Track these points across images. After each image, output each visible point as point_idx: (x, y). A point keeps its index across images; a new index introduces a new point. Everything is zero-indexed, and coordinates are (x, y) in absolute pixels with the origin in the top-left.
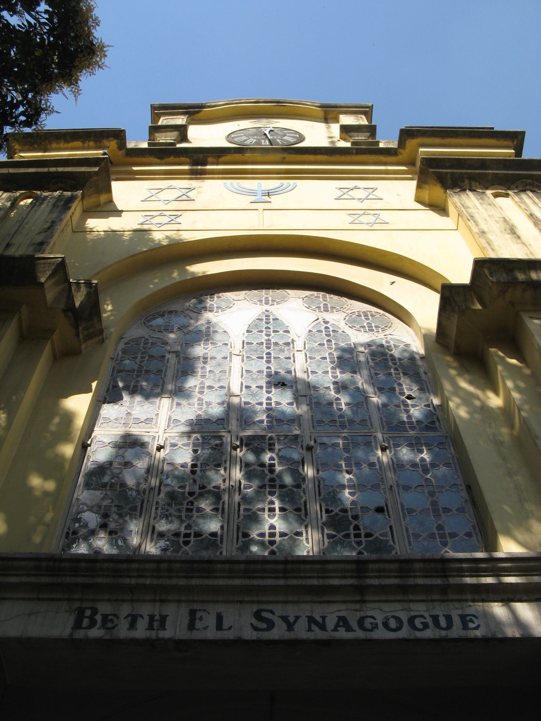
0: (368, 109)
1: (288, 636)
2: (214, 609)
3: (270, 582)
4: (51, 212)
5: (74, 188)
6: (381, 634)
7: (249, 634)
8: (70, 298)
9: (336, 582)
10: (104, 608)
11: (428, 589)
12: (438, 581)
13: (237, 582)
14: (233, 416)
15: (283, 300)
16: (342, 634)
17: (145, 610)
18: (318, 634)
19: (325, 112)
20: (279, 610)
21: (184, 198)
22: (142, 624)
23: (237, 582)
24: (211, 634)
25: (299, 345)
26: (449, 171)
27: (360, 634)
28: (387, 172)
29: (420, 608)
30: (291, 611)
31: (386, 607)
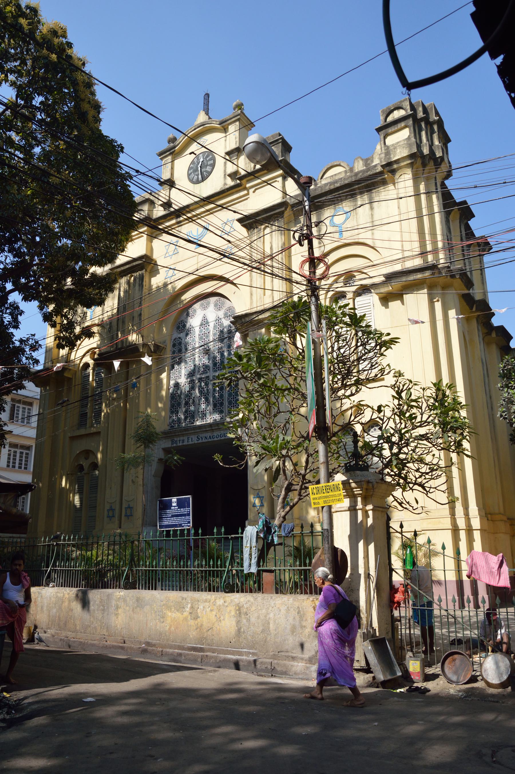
2: (191, 437)
3: (198, 431)
4: (139, 290)
5: (141, 269)
6: (216, 439)
7: (196, 442)
8: (150, 349)
10: (175, 439)
14: (197, 369)
15: (208, 304)
16: (210, 440)
17: (181, 438)
18: (206, 440)
20: (200, 435)
22: (181, 442)
24: (191, 443)
25: (211, 333)
26: (247, 222)
27: (212, 440)
30: (203, 435)
31: (217, 432)
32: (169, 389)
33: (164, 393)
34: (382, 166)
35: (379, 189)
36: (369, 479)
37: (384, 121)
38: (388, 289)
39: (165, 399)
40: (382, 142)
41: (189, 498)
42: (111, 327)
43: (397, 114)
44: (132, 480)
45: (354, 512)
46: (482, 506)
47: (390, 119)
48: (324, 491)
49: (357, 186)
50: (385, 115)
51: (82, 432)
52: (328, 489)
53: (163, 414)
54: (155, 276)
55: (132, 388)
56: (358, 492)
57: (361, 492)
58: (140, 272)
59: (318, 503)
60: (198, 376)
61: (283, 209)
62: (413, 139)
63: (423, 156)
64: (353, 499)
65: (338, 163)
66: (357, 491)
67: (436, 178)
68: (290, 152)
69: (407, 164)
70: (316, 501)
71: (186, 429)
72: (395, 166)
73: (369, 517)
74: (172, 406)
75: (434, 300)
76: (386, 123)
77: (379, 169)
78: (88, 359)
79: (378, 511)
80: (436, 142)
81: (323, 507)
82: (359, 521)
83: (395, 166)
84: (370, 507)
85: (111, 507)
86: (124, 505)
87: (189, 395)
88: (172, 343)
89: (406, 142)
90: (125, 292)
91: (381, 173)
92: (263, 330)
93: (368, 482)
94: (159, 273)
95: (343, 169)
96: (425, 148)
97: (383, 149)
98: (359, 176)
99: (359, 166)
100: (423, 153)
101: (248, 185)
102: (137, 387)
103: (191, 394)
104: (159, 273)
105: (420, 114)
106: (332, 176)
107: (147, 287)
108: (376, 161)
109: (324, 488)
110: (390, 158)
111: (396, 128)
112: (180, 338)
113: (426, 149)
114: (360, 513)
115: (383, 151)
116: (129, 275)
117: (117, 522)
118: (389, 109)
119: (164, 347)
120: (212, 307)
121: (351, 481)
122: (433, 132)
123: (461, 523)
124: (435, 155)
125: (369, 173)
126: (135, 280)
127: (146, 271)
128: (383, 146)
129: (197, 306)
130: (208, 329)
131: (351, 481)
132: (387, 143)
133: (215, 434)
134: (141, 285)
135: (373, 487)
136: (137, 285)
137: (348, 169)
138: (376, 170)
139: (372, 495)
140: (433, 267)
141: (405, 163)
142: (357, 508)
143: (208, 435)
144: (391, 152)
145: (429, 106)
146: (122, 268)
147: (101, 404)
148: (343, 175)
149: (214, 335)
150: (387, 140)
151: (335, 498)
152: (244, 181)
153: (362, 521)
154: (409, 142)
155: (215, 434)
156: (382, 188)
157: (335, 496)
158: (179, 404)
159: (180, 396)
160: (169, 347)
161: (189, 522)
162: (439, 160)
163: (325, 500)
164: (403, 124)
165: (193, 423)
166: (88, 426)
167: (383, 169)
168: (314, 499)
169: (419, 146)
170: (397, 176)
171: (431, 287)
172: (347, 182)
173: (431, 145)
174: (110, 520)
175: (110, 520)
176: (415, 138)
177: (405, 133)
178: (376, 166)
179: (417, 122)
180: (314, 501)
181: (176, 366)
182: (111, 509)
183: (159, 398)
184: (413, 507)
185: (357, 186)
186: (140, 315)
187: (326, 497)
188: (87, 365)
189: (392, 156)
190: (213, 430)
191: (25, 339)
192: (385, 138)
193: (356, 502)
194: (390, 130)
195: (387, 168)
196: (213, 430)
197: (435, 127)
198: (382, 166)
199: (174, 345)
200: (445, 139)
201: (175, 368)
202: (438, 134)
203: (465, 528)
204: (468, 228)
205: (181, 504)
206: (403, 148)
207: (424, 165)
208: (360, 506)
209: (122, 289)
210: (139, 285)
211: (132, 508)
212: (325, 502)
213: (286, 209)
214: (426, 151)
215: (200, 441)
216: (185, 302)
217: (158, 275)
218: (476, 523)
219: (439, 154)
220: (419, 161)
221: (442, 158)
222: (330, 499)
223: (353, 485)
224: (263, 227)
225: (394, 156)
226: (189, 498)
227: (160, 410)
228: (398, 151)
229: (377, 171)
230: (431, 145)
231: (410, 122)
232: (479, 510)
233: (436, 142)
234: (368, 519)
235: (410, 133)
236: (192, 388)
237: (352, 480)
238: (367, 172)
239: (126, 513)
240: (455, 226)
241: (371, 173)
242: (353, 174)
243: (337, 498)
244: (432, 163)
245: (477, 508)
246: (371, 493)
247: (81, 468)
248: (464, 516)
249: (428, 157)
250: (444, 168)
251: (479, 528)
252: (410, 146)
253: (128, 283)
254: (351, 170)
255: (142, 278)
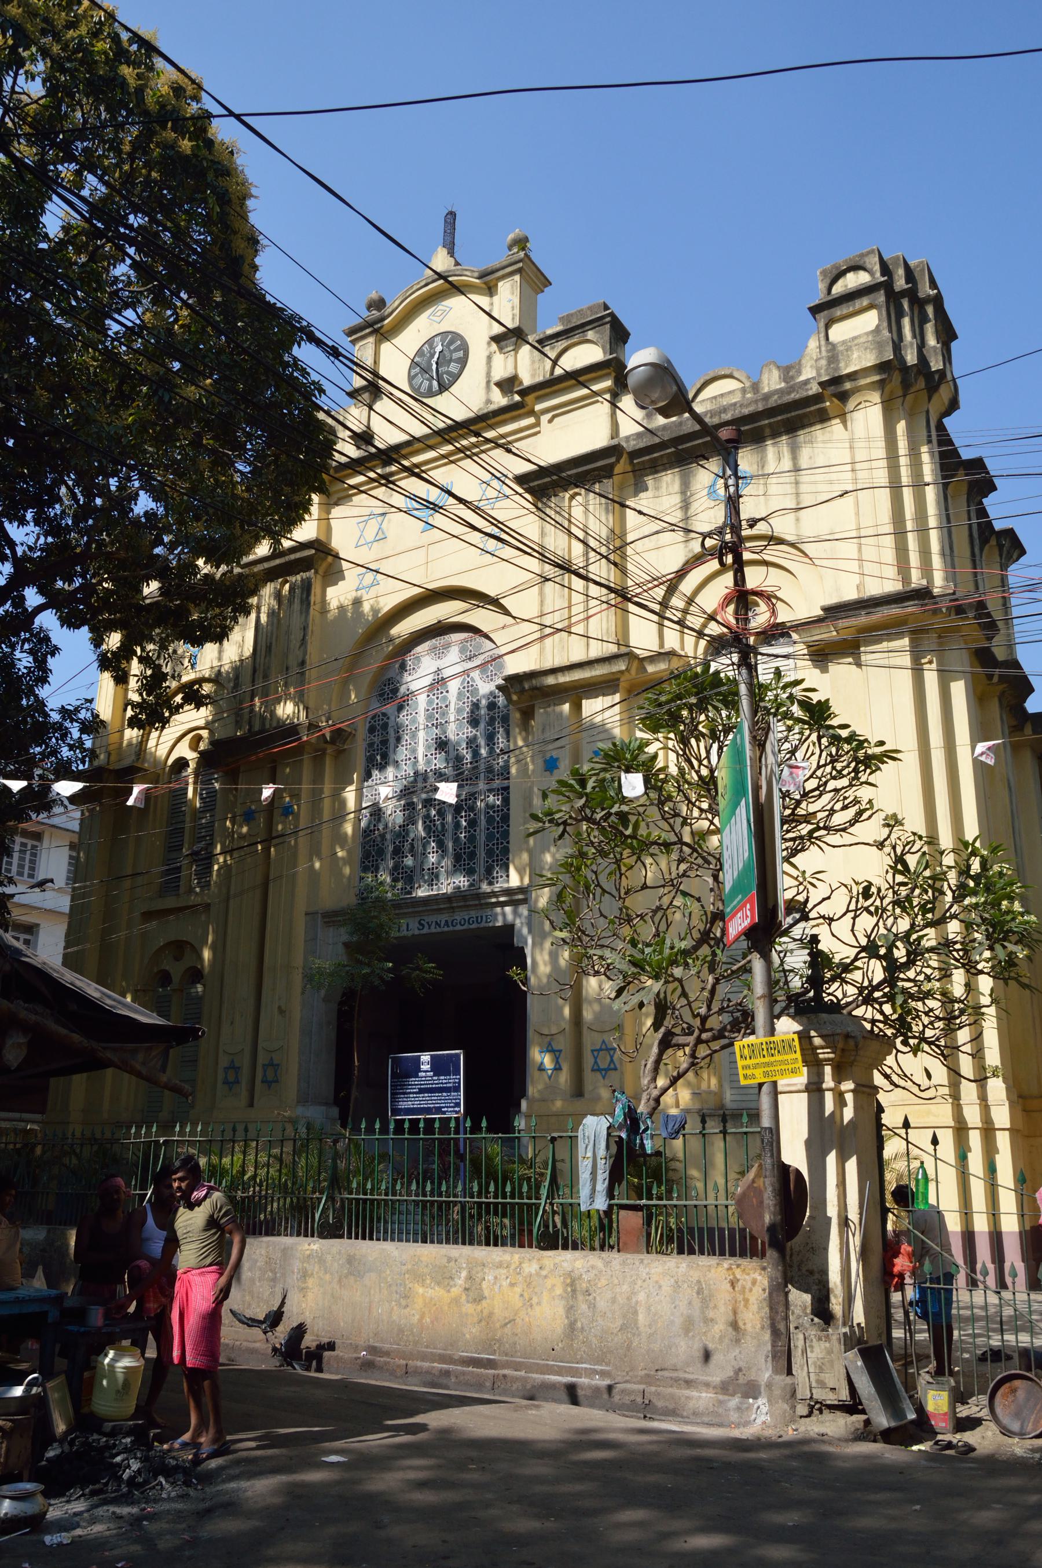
0: (521, 265)
1: (429, 931)
3: (421, 909)
4: (301, 613)
5: (307, 569)
6: (459, 928)
7: (417, 932)
9: (442, 906)
11: (476, 905)
12: (477, 902)
13: (410, 910)
15: (447, 646)
16: (446, 929)
18: (439, 930)
19: (485, 283)
21: (380, 536)
23: (410, 910)
25: (452, 706)
27: (451, 928)
28: (521, 430)
29: (473, 914)
30: (432, 919)
32: (360, 820)
33: (349, 828)
34: (821, 384)
35: (813, 429)
36: (849, 1029)
37: (825, 292)
38: (828, 633)
39: (350, 841)
40: (822, 335)
41: (458, 1055)
42: (237, 686)
43: (853, 280)
44: (279, 1007)
45: (816, 1094)
46: (1011, 1083)
47: (838, 289)
48: (765, 1052)
49: (767, 422)
50: (828, 281)
51: (170, 902)
52: (772, 1049)
53: (347, 871)
54: (336, 584)
55: (283, 815)
56: (826, 1056)
57: (832, 1056)
58: (304, 575)
59: (753, 1076)
60: (424, 796)
61: (613, 460)
62: (886, 333)
63: (904, 368)
64: (814, 1069)
65: (728, 372)
66: (824, 1054)
67: (928, 412)
68: (625, 342)
69: (873, 383)
70: (749, 1072)
71: (397, 905)
72: (848, 386)
73: (846, 1105)
74: (366, 855)
75: (923, 661)
76: (830, 298)
77: (814, 389)
78: (184, 750)
79: (863, 1092)
80: (931, 341)
81: (761, 1085)
82: (827, 1114)
83: (848, 386)
84: (848, 1085)
85: (233, 1061)
86: (261, 1060)
87: (403, 832)
88: (368, 725)
89: (870, 338)
90: (271, 614)
91: (818, 398)
92: (566, 707)
93: (847, 1036)
94: (343, 578)
95: (740, 385)
96: (909, 351)
97: (823, 349)
98: (773, 402)
99: (772, 381)
100: (904, 362)
101: (538, 408)
102: (292, 813)
103: (407, 834)
104: (343, 578)
105: (900, 283)
106: (715, 398)
107: (318, 607)
108: (807, 373)
109: (764, 1046)
110: (837, 369)
111: (851, 309)
112: (384, 714)
113: (912, 353)
114: (829, 1097)
115: (824, 354)
116: (280, 580)
117: (244, 1094)
118: (837, 268)
119: (351, 733)
120: (454, 655)
121: (813, 1033)
122: (924, 320)
123: (972, 1115)
124: (930, 367)
125: (792, 395)
126: (292, 589)
127: (316, 572)
128: (823, 342)
129: (421, 649)
130: (445, 698)
131: (813, 1033)
132: (831, 338)
133: (458, 918)
134: (306, 602)
135: (856, 1046)
136: (297, 601)
137: (748, 384)
138: (807, 390)
139: (855, 1060)
140: (923, 594)
141: (868, 380)
142: (824, 1086)
143: (443, 918)
144: (840, 357)
145: (918, 266)
146: (266, 565)
147: (212, 845)
148: (736, 398)
149: (459, 711)
150: (831, 332)
151: (786, 1067)
152: (530, 399)
153: (833, 1114)
154: (878, 339)
155: (458, 918)
156: (818, 427)
157: (785, 1062)
158: (381, 852)
159: (383, 836)
160: (362, 733)
161: (458, 1105)
162: (937, 377)
163: (766, 1069)
164: (865, 301)
165: (410, 893)
166: (182, 890)
167: (823, 389)
168: (744, 1067)
169: (897, 346)
170: (851, 404)
171: (917, 635)
172: (746, 411)
173: (922, 345)
174: (230, 1089)
175: (230, 1089)
176: (890, 331)
177: (869, 321)
178: (806, 382)
179: (893, 297)
180: (745, 1072)
181: (376, 773)
182: (233, 1067)
183: (340, 838)
184: (919, 1086)
185: (767, 422)
186: (303, 663)
187: (768, 1064)
188: (181, 763)
189: (842, 365)
190: (452, 909)
191: (71, 708)
192: (827, 327)
193: (821, 1076)
194: (838, 312)
195: (832, 389)
196: (453, 908)
197: (930, 310)
198: (821, 384)
199: (372, 730)
200: (947, 334)
201: (374, 777)
202: (936, 325)
203: (980, 1125)
204: (983, 513)
205: (439, 1067)
206: (866, 349)
207: (906, 385)
208: (829, 1082)
209: (264, 609)
210: (302, 602)
211: (278, 1065)
212: (766, 1074)
213: (618, 461)
214: (911, 358)
215: (425, 931)
216: (397, 641)
217: (340, 583)
218: (1002, 1116)
219: (936, 364)
220: (897, 377)
221: (942, 373)
222: (776, 1068)
223: (818, 1041)
224: (567, 496)
225: (847, 366)
226: (458, 1055)
227: (341, 863)
228: (855, 355)
229: (810, 393)
230: (922, 345)
231: (881, 298)
232: (1007, 1089)
233: (931, 341)
234: (845, 1109)
235: (880, 320)
236: (410, 820)
237: (815, 1031)
238: (789, 393)
239: (265, 1075)
240: (960, 508)
241: (798, 396)
242: (759, 396)
243: (790, 1067)
244: (921, 383)
245: (1004, 1086)
246: (852, 1058)
247: (165, 978)
248: (978, 1102)
249: (915, 370)
250: (944, 393)
251: (1008, 1126)
252: (879, 346)
253: (278, 595)
254: (755, 387)
255: (307, 586)
